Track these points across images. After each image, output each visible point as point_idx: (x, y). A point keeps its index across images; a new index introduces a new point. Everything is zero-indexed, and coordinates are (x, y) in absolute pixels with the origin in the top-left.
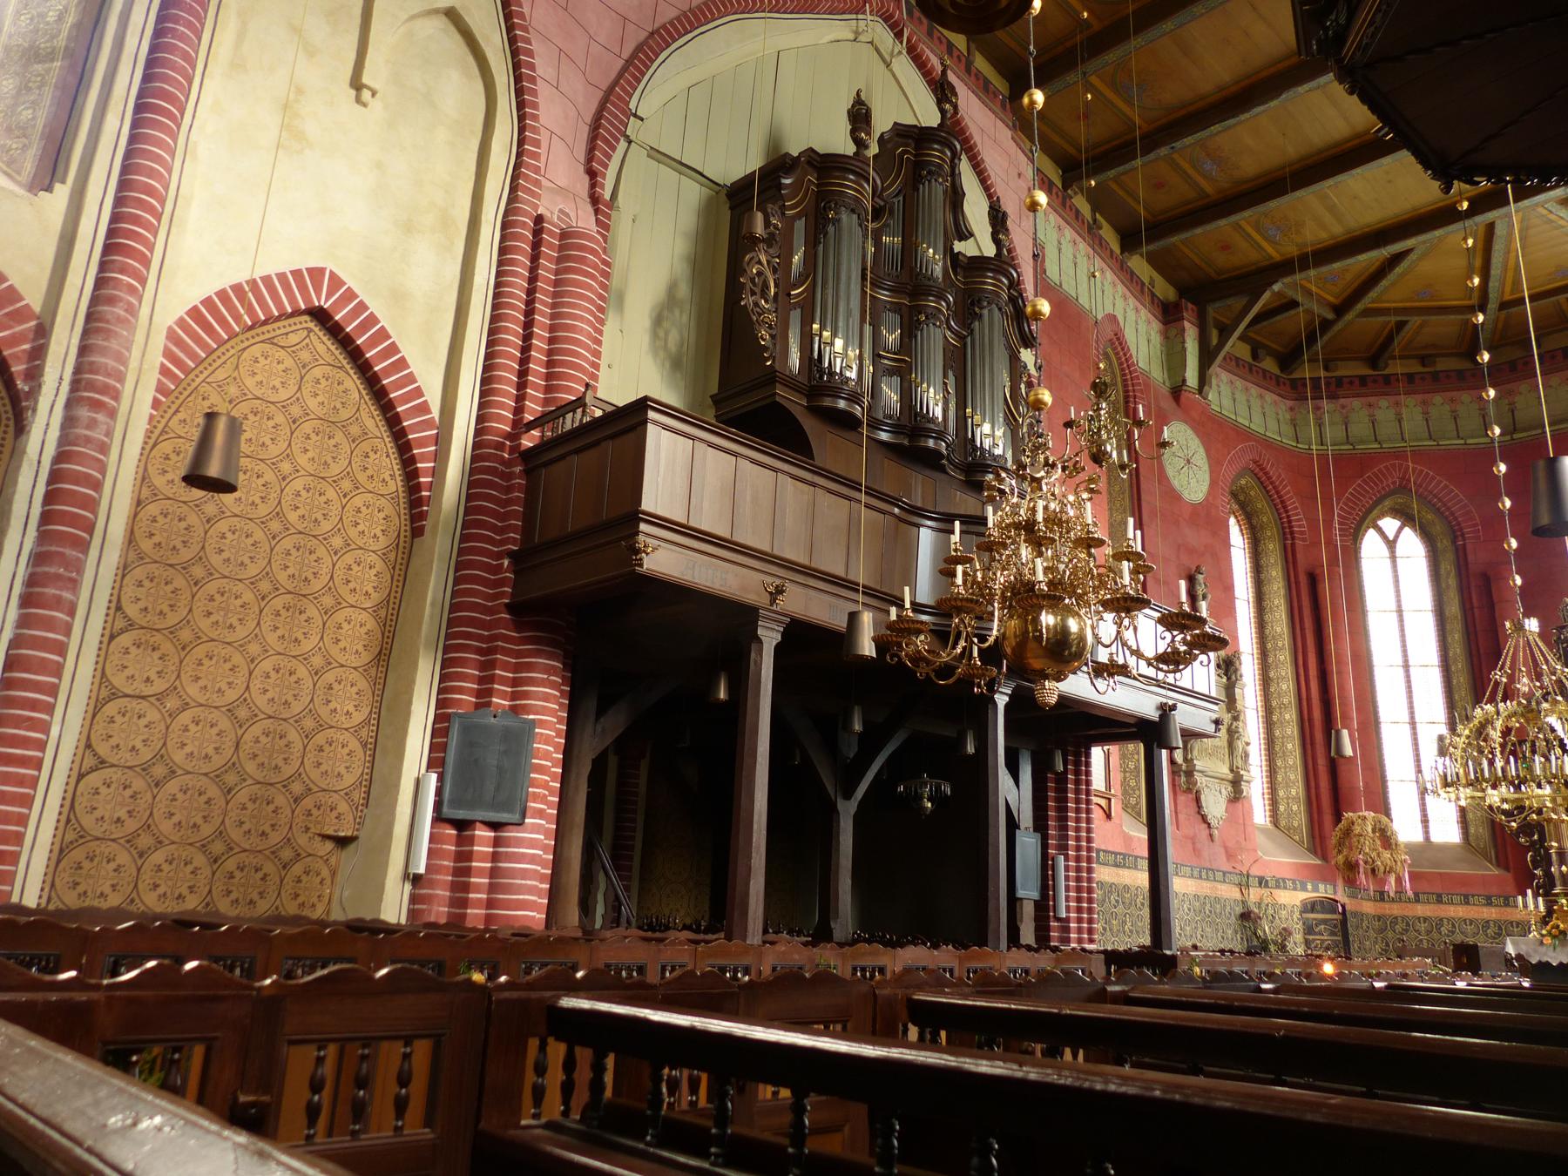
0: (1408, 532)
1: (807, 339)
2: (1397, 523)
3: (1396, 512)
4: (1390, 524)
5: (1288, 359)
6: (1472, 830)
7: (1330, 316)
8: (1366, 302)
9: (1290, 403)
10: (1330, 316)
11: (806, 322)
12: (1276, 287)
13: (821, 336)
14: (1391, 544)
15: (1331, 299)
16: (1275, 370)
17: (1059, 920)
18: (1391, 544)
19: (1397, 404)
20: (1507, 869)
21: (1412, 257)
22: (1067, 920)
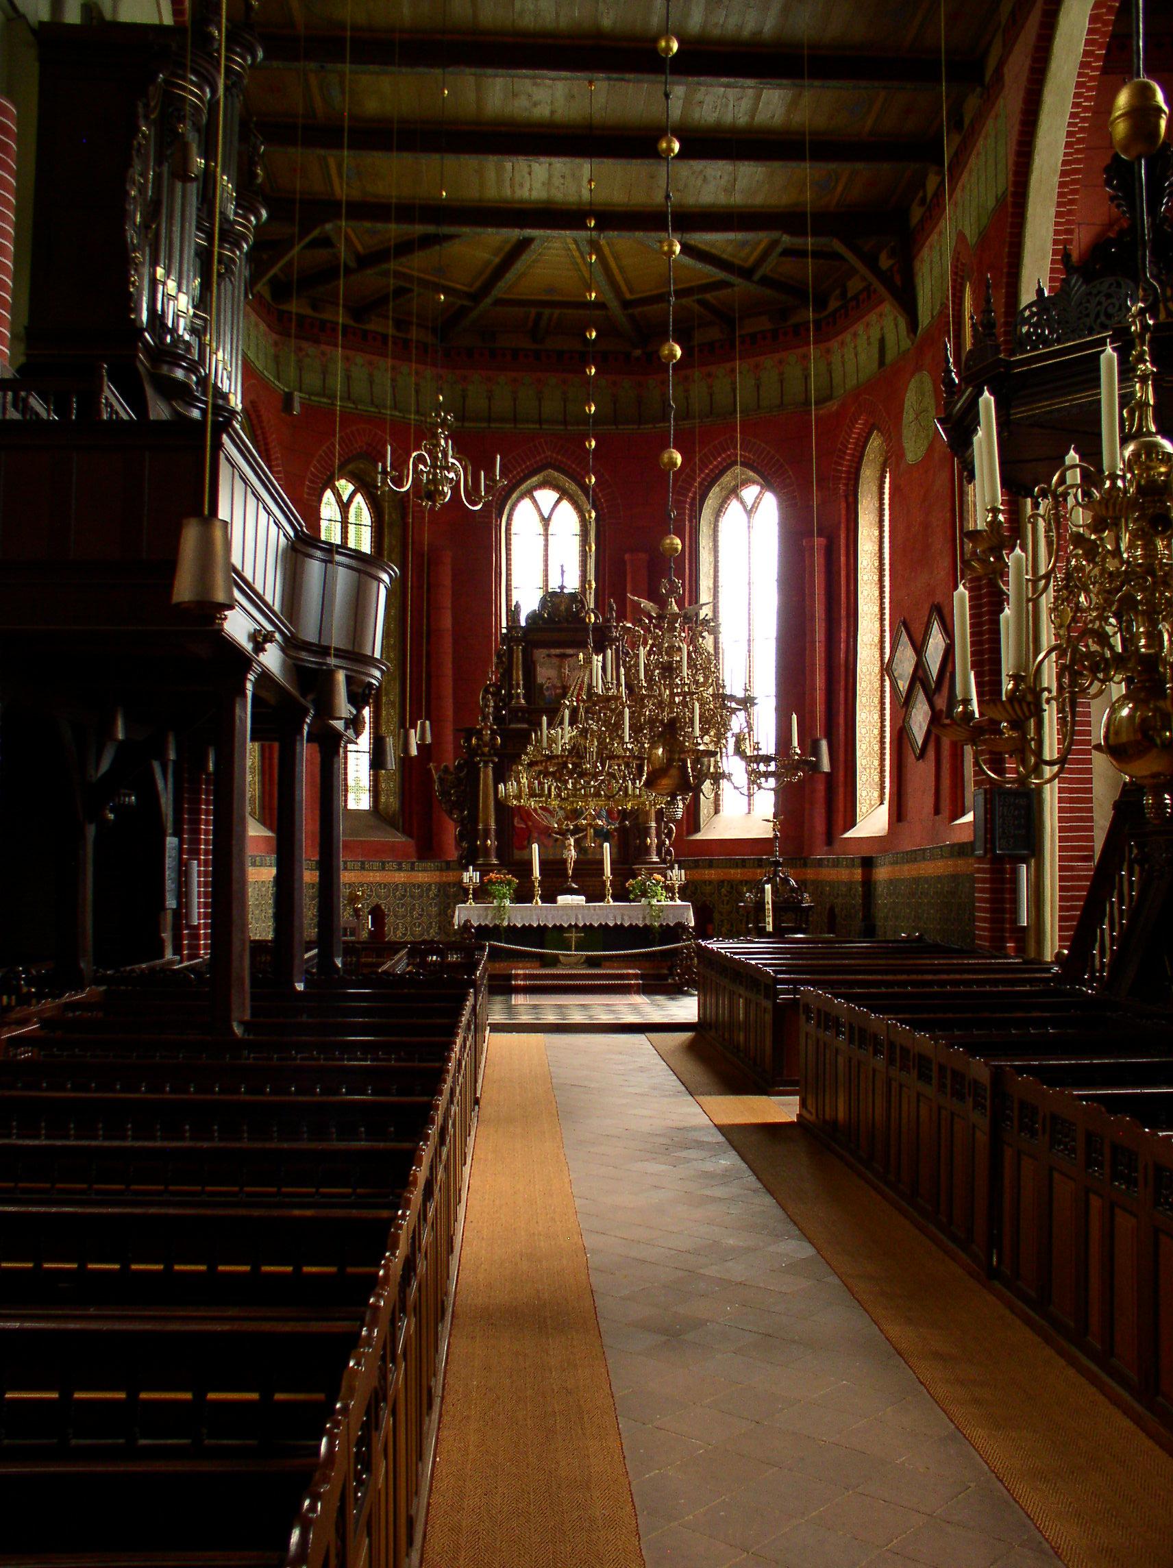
0: (359, 498)
1: (154, 282)
2: (351, 488)
3: (352, 478)
4: (346, 487)
5: (281, 290)
6: (383, 799)
7: (352, 264)
8: (392, 265)
9: (275, 336)
10: (352, 264)
11: (154, 263)
12: (328, 226)
13: (164, 284)
14: (344, 507)
15: (360, 248)
16: (268, 296)
17: (189, 927)
18: (344, 507)
19: (370, 363)
20: (410, 835)
21: (457, 241)
22: (198, 927)
